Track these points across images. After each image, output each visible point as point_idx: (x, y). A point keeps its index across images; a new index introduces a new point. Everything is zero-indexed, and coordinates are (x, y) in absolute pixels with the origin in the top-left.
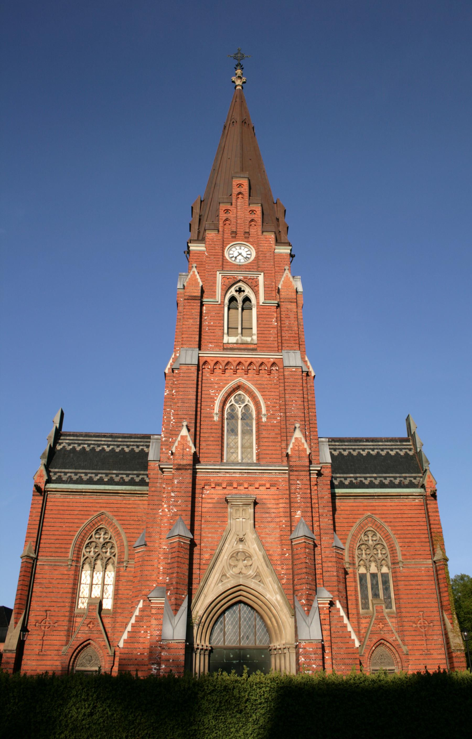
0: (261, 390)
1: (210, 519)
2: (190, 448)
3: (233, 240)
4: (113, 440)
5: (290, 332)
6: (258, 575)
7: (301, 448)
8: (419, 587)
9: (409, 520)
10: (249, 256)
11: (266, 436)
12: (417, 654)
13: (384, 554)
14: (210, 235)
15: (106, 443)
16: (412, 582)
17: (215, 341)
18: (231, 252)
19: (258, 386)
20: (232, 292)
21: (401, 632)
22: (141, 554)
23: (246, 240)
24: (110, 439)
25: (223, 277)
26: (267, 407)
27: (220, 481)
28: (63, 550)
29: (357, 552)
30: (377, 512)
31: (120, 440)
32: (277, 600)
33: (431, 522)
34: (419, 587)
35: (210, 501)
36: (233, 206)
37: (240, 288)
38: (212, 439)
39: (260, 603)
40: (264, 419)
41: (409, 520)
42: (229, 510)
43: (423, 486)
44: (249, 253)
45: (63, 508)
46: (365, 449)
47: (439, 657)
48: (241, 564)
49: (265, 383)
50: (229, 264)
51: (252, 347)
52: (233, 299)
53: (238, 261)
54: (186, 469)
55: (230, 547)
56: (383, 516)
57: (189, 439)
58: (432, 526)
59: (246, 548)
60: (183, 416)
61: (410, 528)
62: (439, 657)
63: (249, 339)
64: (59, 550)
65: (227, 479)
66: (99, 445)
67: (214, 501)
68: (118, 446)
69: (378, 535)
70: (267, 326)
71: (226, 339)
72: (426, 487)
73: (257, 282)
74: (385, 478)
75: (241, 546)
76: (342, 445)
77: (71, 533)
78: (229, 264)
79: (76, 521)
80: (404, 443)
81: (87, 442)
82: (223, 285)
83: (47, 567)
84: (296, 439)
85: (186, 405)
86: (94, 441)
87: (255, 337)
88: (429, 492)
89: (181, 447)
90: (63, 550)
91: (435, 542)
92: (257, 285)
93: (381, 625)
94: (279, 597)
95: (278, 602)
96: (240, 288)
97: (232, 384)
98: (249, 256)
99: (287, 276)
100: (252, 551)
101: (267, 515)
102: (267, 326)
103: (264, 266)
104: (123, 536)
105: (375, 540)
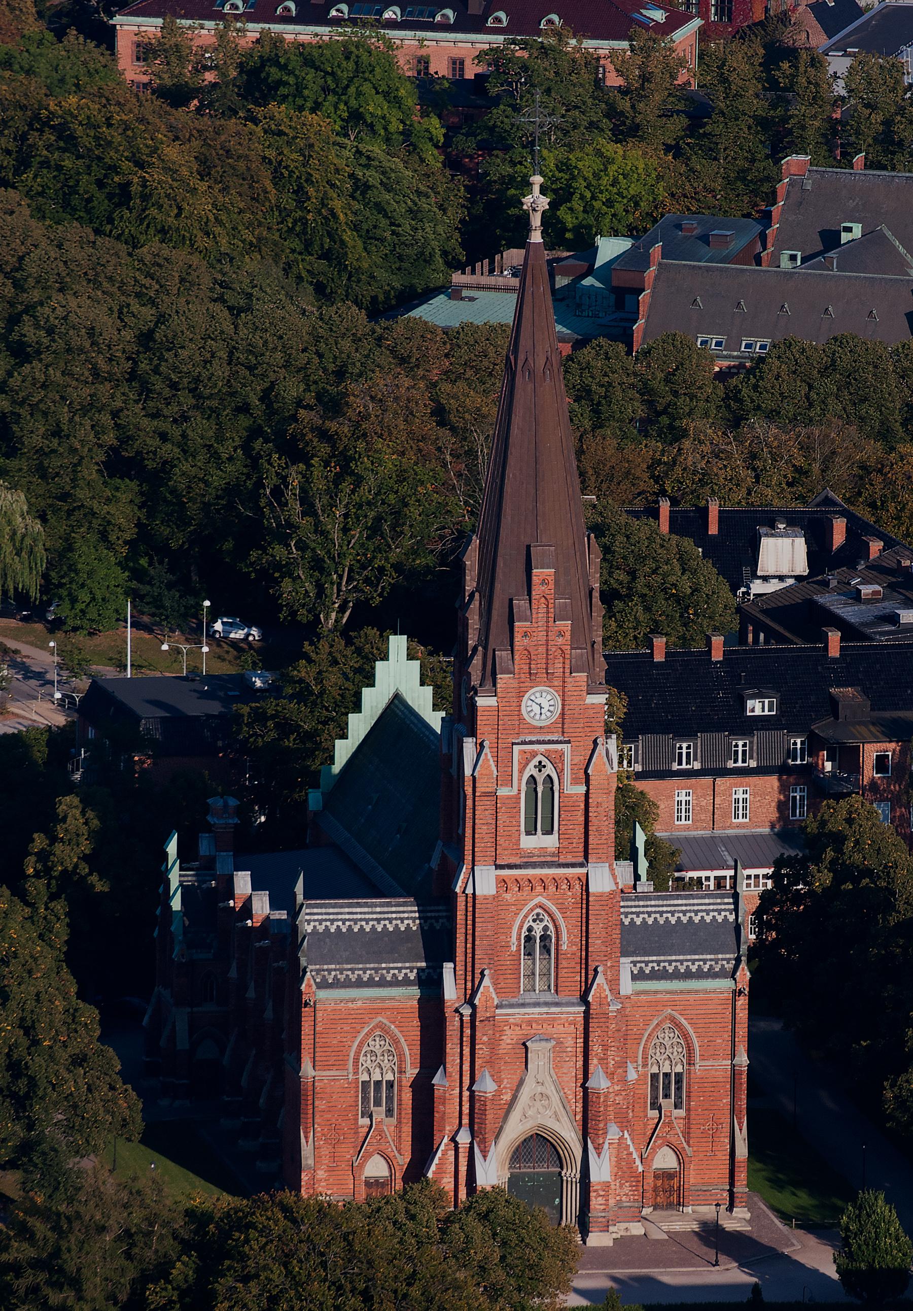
0: (562, 910)
10: (552, 708)
12: (701, 1155)
15: (363, 916)
20: (531, 770)
21: (687, 1134)
29: (651, 1052)
30: (677, 1008)
37: (540, 762)
40: (564, 947)
44: (552, 703)
48: (538, 1104)
57: (492, 989)
68: (378, 920)
74: (693, 962)
75: (539, 1089)
76: (647, 906)
81: (340, 917)
82: (520, 763)
86: (349, 913)
89: (484, 998)
93: (667, 1129)
94: (573, 1134)
96: (540, 762)
97: (531, 904)
100: (550, 1093)
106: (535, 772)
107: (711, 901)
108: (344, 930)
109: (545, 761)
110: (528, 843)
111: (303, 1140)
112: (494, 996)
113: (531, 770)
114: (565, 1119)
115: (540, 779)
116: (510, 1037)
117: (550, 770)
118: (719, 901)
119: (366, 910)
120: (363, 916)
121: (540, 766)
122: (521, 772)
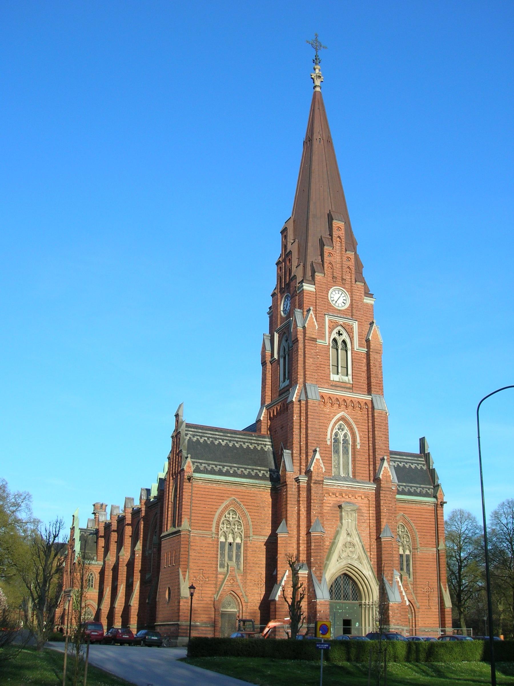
1: (328, 518)
2: (322, 468)
3: (334, 284)
4: (224, 434)
5: (377, 379)
6: (359, 558)
7: (388, 475)
8: (427, 566)
9: (425, 520)
11: (360, 459)
13: (409, 542)
14: (318, 276)
16: (424, 562)
17: (325, 378)
18: (332, 296)
19: (354, 420)
22: (282, 539)
23: (343, 286)
24: (222, 434)
25: (330, 321)
26: (360, 437)
27: (335, 492)
28: (208, 525)
31: (229, 435)
32: (369, 575)
33: (439, 523)
34: (427, 566)
35: (328, 505)
36: (334, 250)
38: (326, 458)
39: (357, 575)
40: (358, 447)
41: (425, 520)
42: (343, 513)
43: (435, 497)
45: (205, 493)
46: (396, 461)
47: (435, 610)
48: (348, 550)
49: (359, 418)
50: (331, 308)
51: (349, 386)
52: (335, 340)
53: (337, 305)
54: (320, 484)
55: (342, 538)
56: (410, 515)
57: (321, 461)
58: (439, 526)
59: (352, 539)
60: (313, 441)
61: (425, 525)
62: (435, 610)
63: (346, 379)
64: (205, 525)
65: (339, 490)
66: (216, 439)
67: (331, 505)
69: (406, 528)
70: (359, 370)
71: (334, 377)
72: (438, 497)
73: (352, 329)
75: (349, 539)
77: (212, 513)
78: (331, 308)
79: (215, 503)
80: (420, 459)
82: (329, 328)
83: (197, 538)
84: (385, 467)
85: (314, 432)
86: (211, 434)
87: (350, 377)
88: (440, 501)
90: (208, 525)
91: (439, 537)
92: (353, 332)
94: (371, 573)
95: (370, 576)
98: (345, 302)
99: (375, 329)
100: (355, 542)
101: (362, 518)
102: (359, 370)
103: (356, 315)
104: (249, 517)
105: (404, 532)
106: (337, 336)
107: (412, 458)
108: (209, 442)
109: (343, 331)
110: (334, 377)
111: (181, 577)
112: (322, 466)
113: (334, 335)
114: (365, 562)
115: (340, 342)
116: (330, 501)
117: (345, 336)
118: (416, 459)
119: (222, 434)
120: (220, 437)
121: (340, 334)
122: (330, 333)
